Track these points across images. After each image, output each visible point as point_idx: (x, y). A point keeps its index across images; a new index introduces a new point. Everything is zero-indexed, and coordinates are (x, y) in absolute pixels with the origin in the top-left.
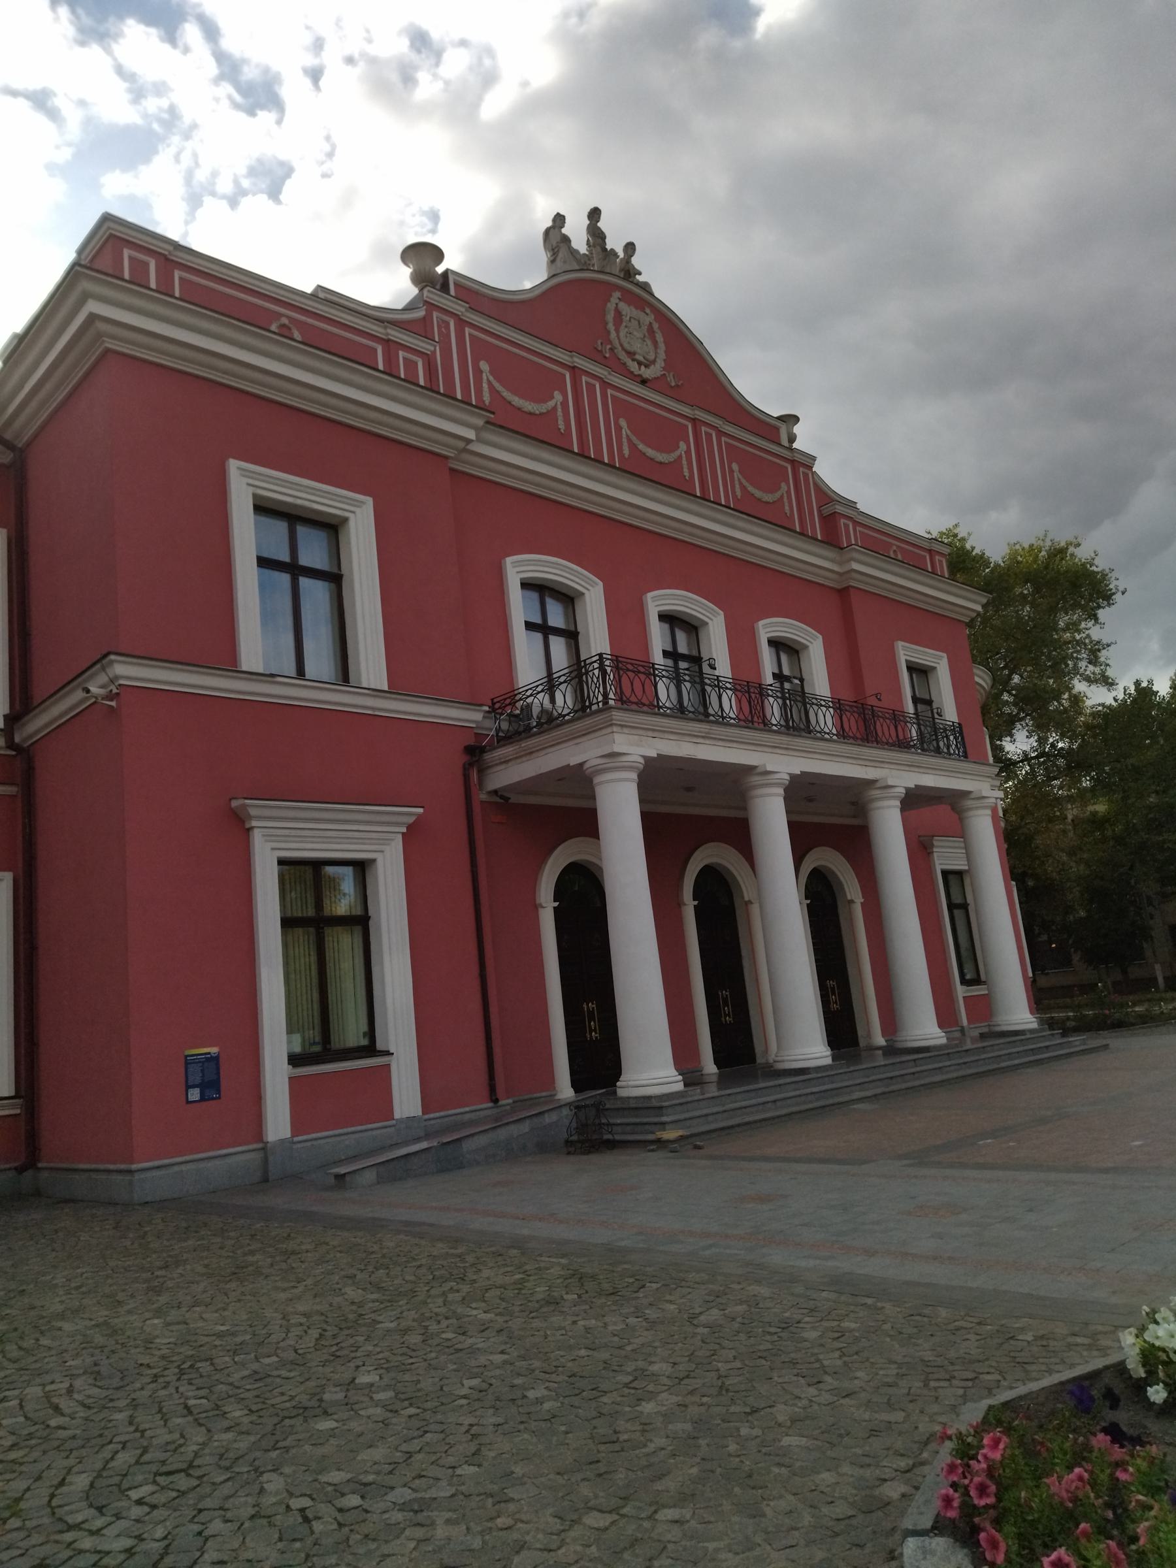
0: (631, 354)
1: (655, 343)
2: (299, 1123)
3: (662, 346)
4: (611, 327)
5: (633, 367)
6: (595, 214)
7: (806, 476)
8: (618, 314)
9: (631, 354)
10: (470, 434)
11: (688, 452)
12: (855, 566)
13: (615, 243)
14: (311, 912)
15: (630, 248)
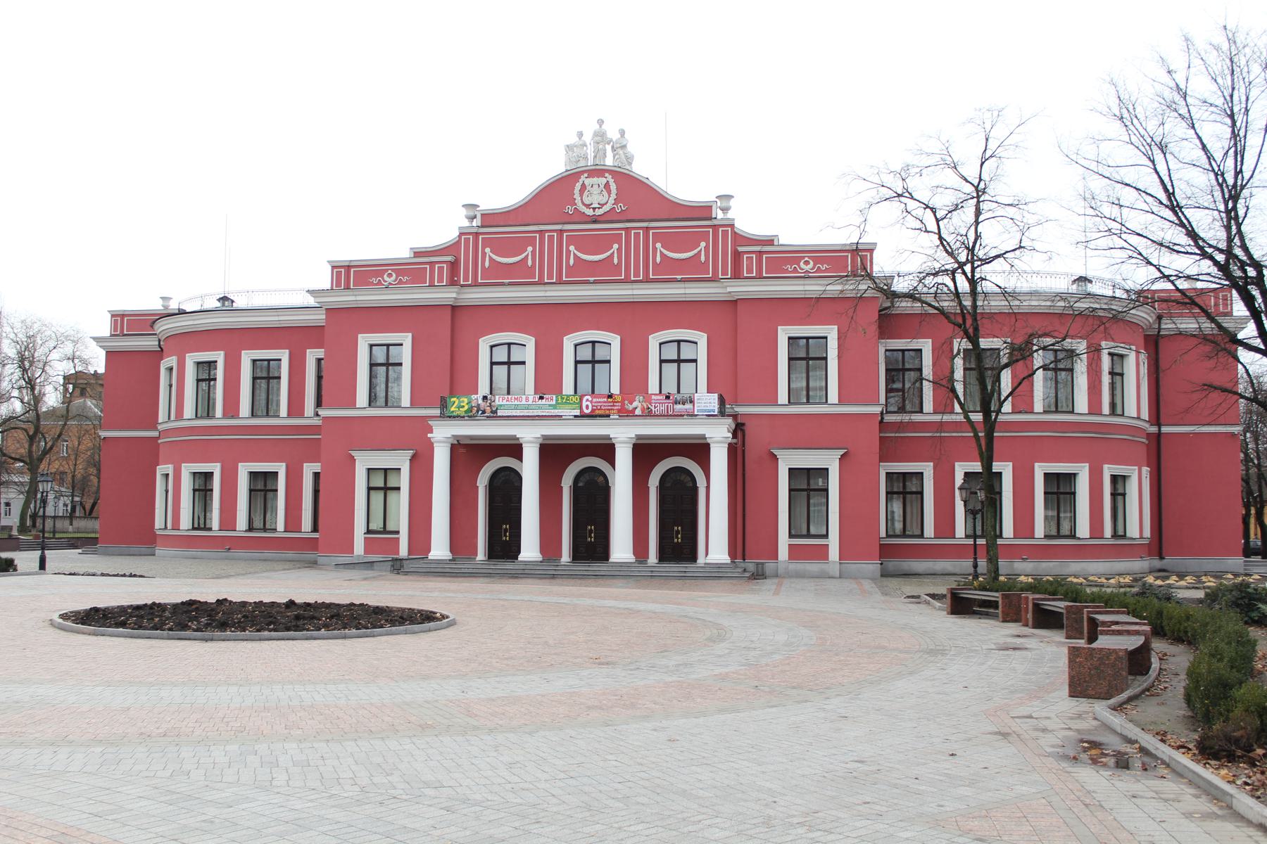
0: (588, 206)
1: (609, 193)
2: (367, 551)
3: (614, 191)
4: (577, 196)
5: (589, 212)
6: (601, 122)
7: (725, 233)
8: (583, 186)
9: (588, 206)
10: (454, 295)
11: (619, 250)
12: (729, 289)
13: (613, 134)
14: (382, 485)
15: (622, 133)
